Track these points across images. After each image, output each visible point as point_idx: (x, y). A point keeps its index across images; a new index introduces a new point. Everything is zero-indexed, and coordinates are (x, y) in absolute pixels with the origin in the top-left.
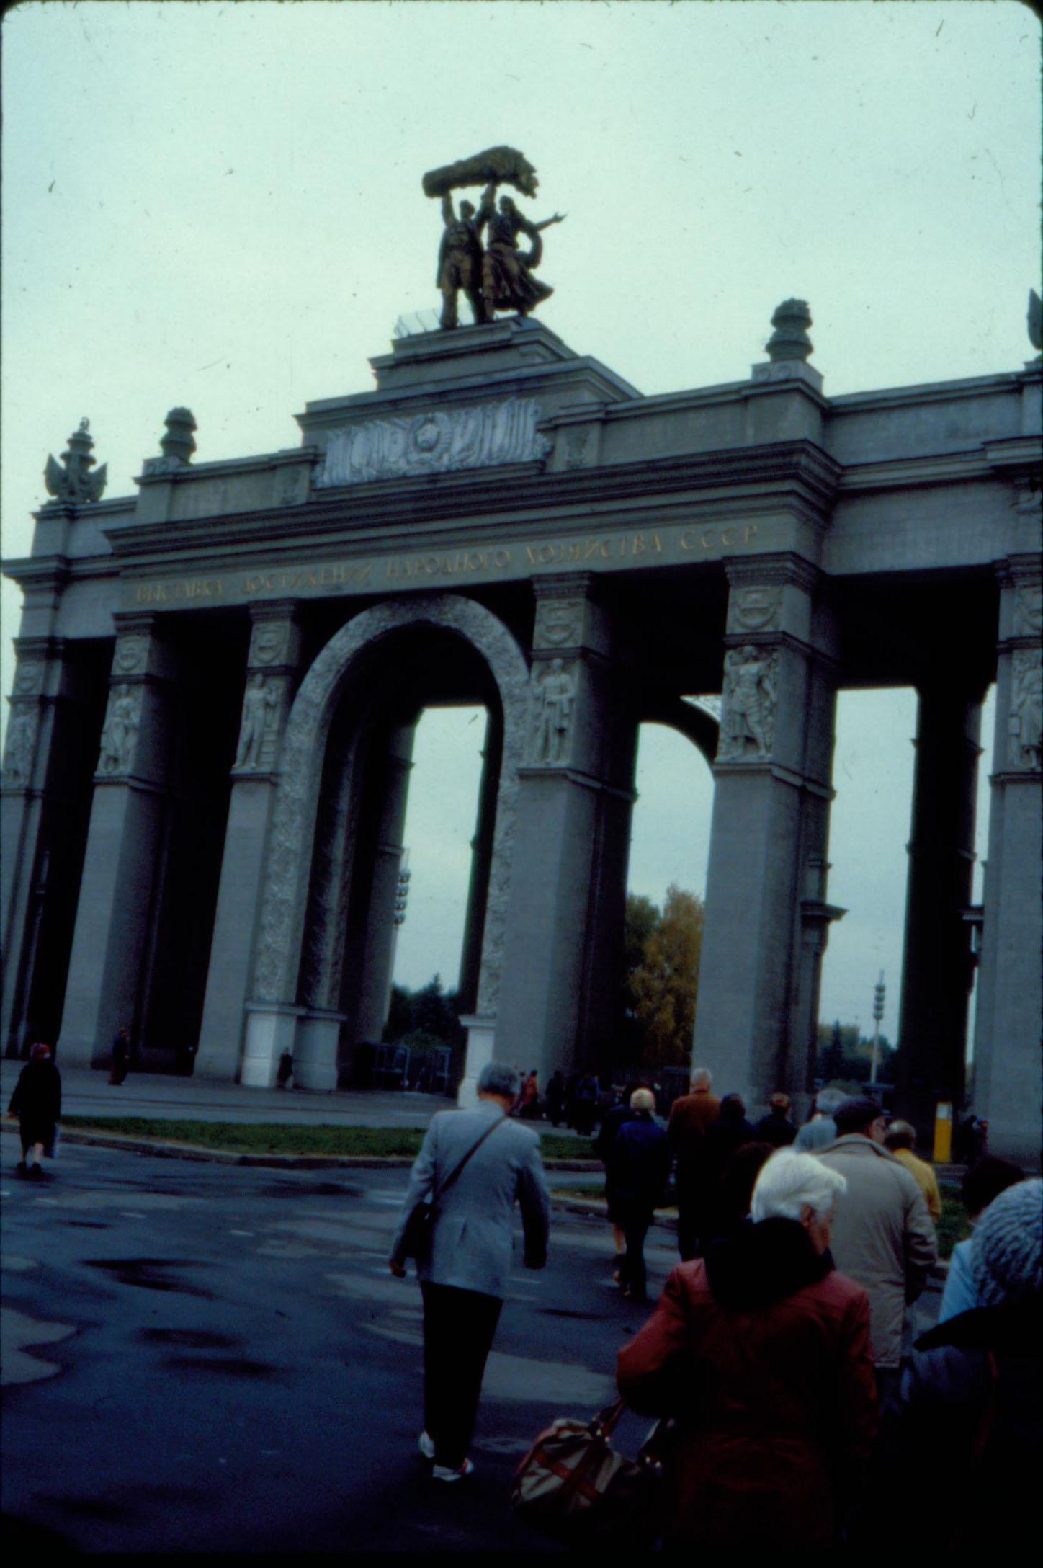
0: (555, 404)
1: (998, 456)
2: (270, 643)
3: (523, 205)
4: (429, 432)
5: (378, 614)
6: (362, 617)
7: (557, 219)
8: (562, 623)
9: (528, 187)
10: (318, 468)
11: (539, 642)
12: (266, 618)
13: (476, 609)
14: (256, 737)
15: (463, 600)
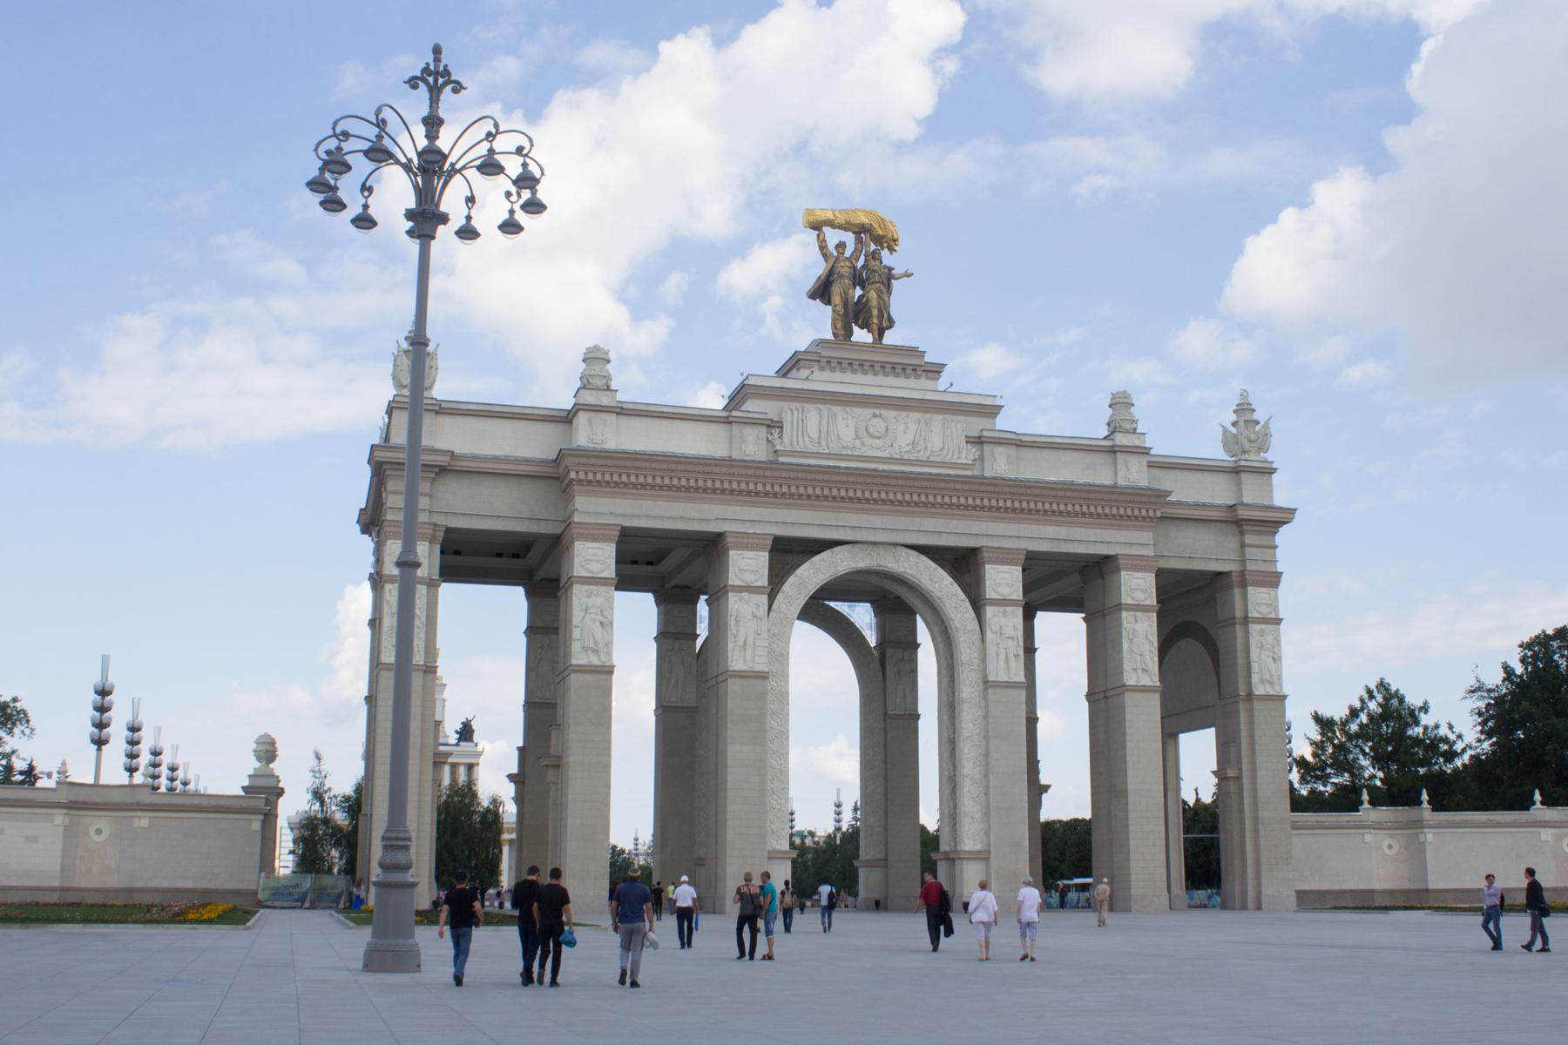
0: (976, 425)
1: (1242, 513)
2: (747, 566)
3: (887, 258)
4: (878, 426)
5: (840, 556)
6: (825, 555)
7: (908, 275)
8: (1003, 581)
9: (891, 250)
10: (776, 432)
11: (990, 592)
12: (747, 547)
13: (925, 562)
14: (750, 642)
15: (914, 553)
